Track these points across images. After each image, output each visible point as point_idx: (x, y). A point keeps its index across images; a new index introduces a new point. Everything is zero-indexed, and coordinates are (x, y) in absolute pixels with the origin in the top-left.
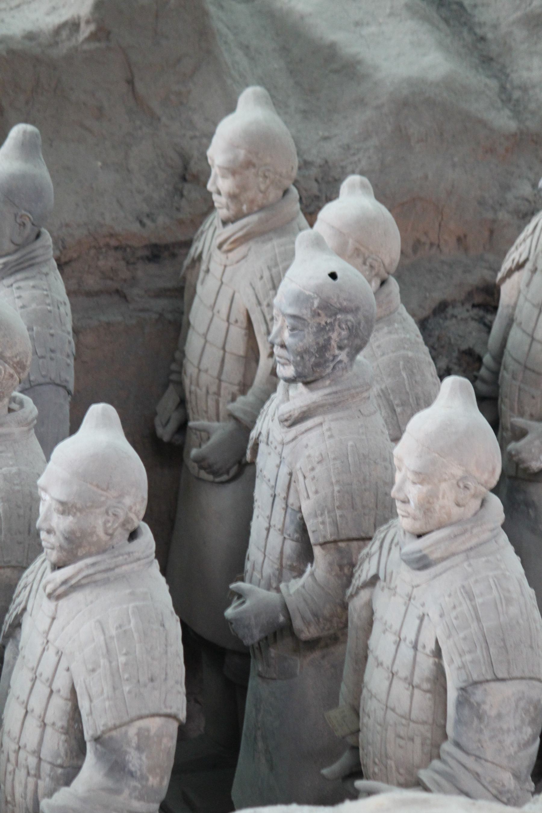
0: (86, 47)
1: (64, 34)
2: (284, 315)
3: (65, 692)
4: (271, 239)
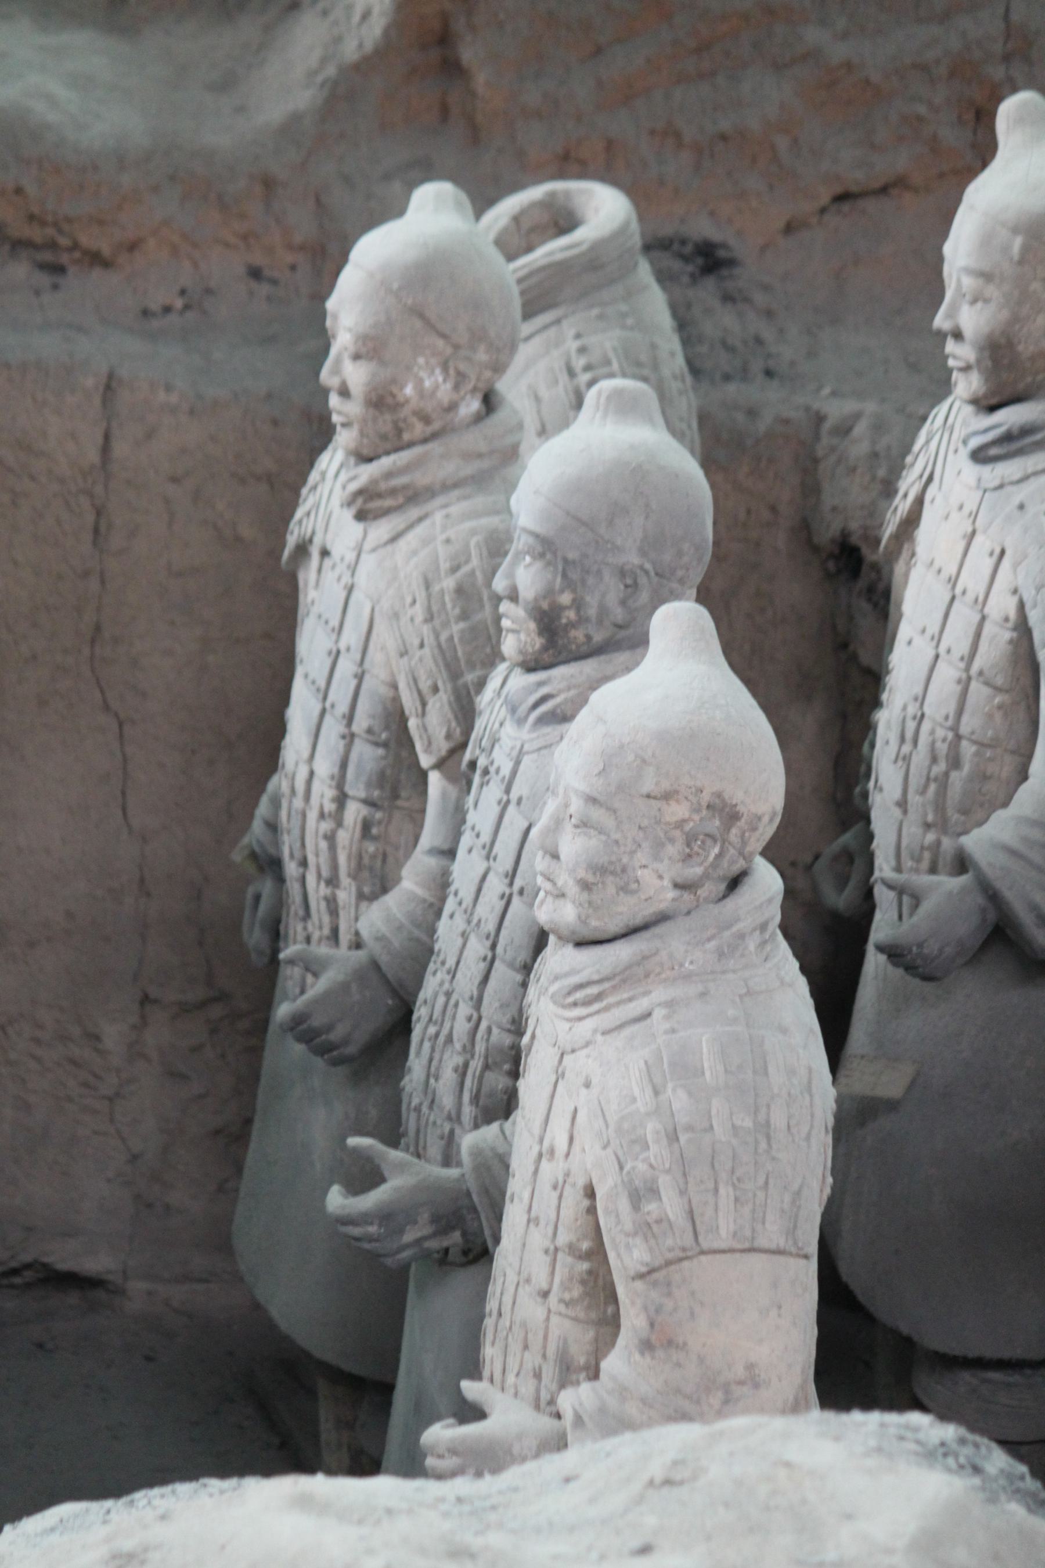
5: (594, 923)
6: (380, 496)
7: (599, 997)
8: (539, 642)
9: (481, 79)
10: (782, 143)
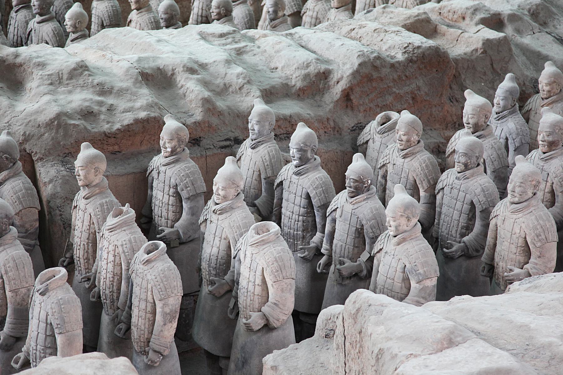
0: (481, 56)
1: (474, 52)
4: (560, 103)
7: (522, 211)
8: (464, 168)
9: (354, 101)
10: (391, 105)
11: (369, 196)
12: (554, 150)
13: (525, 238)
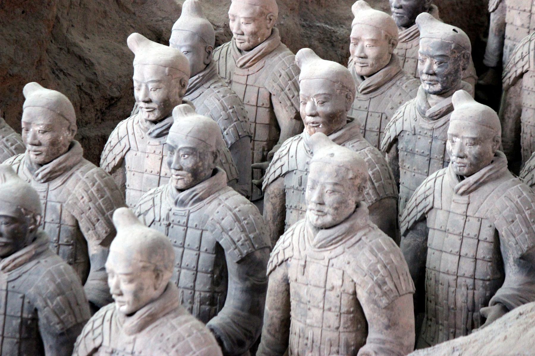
2: (432, 57)
3: (490, 238)
5: (338, 219)
6: (56, 172)
8: (191, 179)
11: (39, 250)
12: (335, 132)
13: (355, 293)
